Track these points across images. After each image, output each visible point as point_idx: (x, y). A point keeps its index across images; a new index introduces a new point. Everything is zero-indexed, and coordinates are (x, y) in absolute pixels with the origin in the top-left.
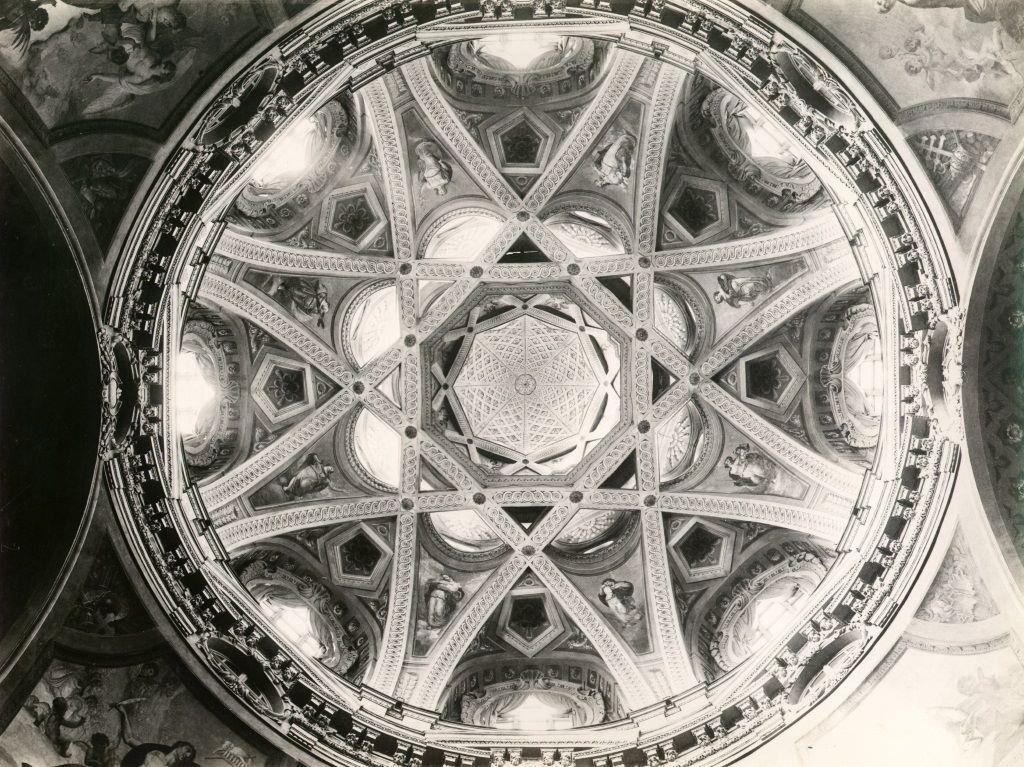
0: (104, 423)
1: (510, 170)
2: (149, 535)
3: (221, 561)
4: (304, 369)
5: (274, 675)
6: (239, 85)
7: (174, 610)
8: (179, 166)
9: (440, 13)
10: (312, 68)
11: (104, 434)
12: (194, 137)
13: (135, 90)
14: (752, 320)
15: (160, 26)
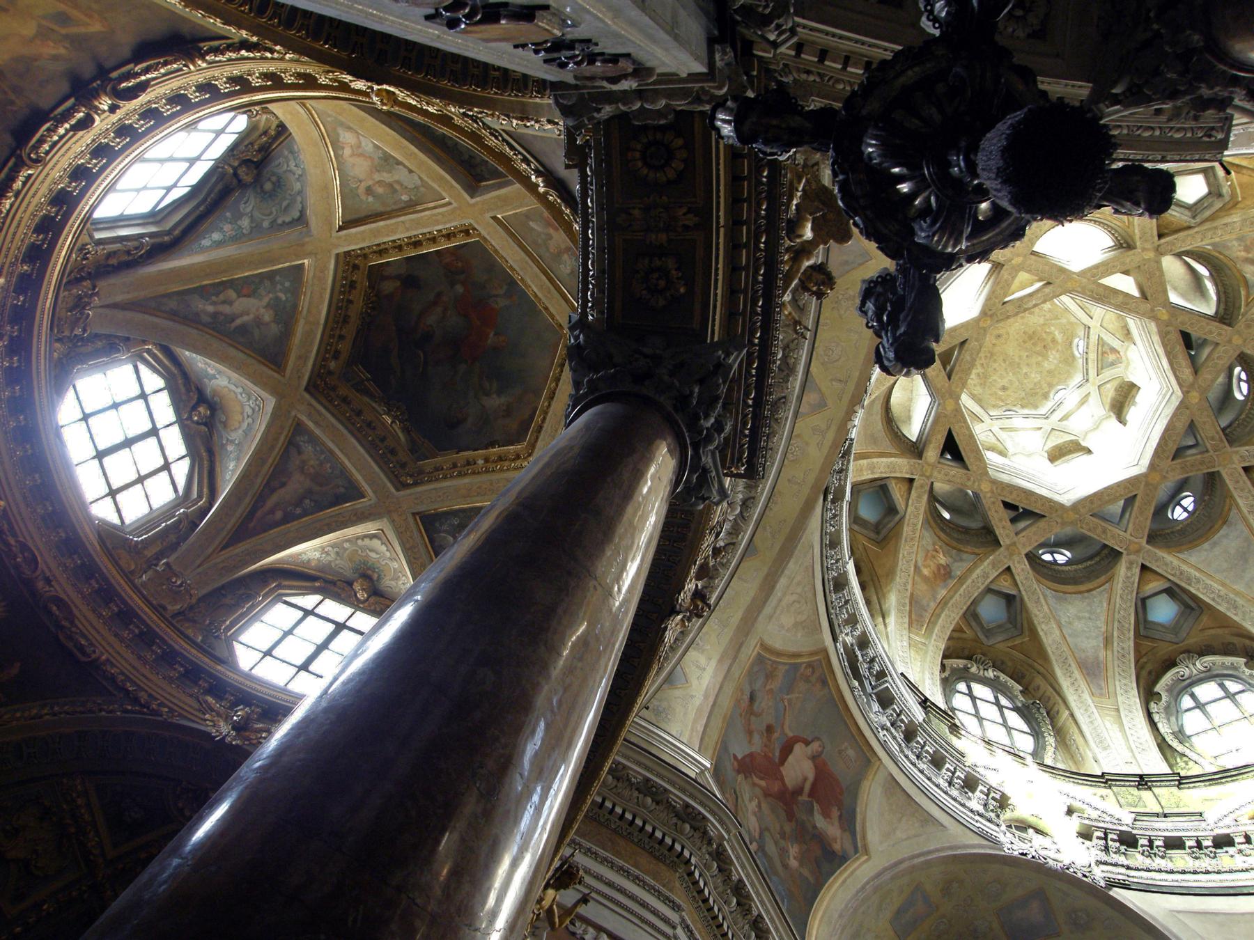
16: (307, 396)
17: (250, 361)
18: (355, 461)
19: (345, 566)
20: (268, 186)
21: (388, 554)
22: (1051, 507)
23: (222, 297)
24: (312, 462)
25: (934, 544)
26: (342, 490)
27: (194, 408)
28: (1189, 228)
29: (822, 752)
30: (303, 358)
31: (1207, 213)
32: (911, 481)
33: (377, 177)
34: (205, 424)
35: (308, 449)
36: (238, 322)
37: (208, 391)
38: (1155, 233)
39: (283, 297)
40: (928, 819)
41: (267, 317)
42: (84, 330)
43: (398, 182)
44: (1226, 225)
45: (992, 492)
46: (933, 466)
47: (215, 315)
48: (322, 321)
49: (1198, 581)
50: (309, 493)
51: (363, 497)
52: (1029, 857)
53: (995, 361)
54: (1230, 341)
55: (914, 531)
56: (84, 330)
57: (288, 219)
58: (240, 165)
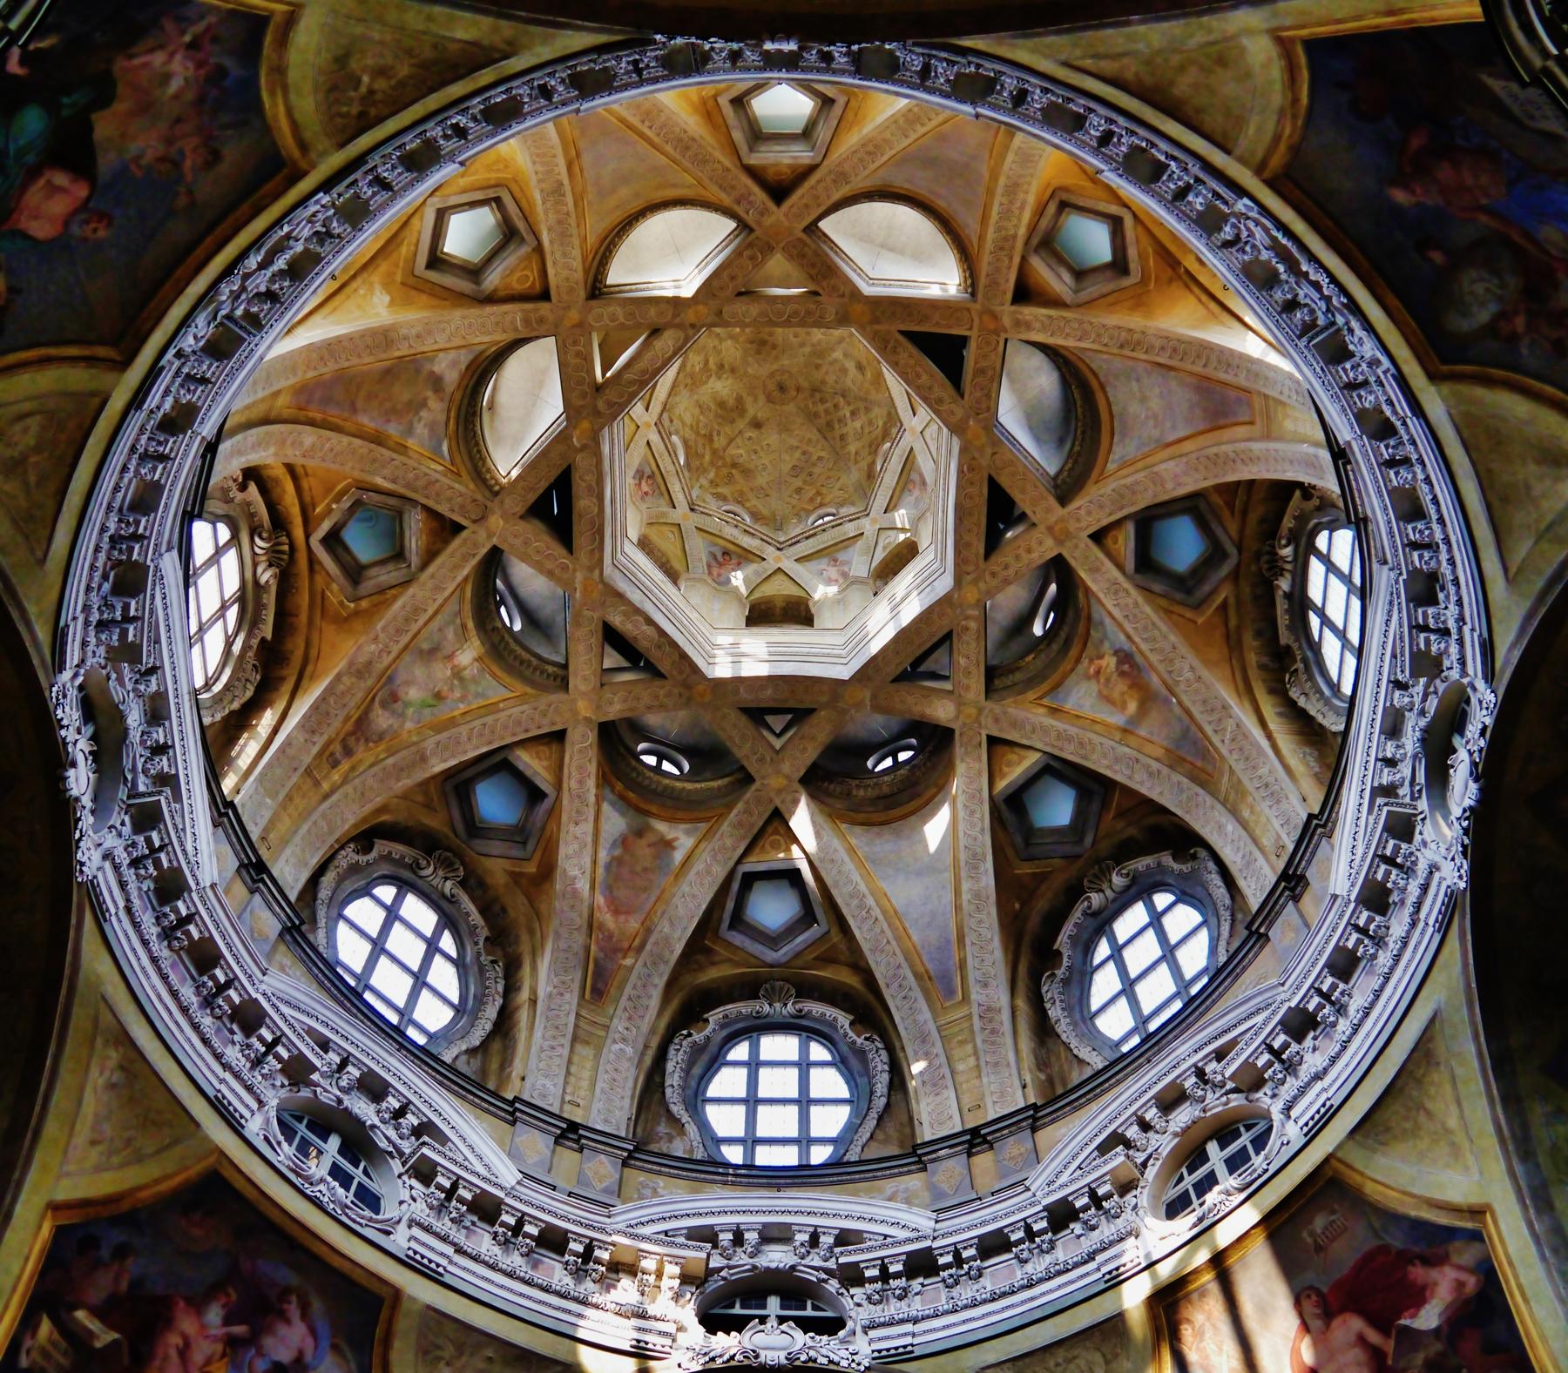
0: (815, 1361)
1: (415, 560)
2: (988, 1284)
3: (1035, 1119)
4: (745, 875)
5: (1216, 1104)
6: (307, 1179)
7: (1098, 1269)
8: (432, 1249)
9: (170, 861)
10: (270, 1047)
11: (831, 1362)
12: (388, 1233)
13: (325, 1344)
14: (669, 148)
15: (227, 1321)
22: (971, 469)
25: (1088, 677)
28: (426, 508)
29: (1319, 1293)
31: (391, 501)
32: (993, 741)
38: (457, 542)
40: (1423, 1051)
44: (394, 482)
45: (975, 582)
46: (960, 704)
49: (999, 229)
52: (1466, 841)
53: (823, 382)
54: (580, 325)
55: (1070, 739)
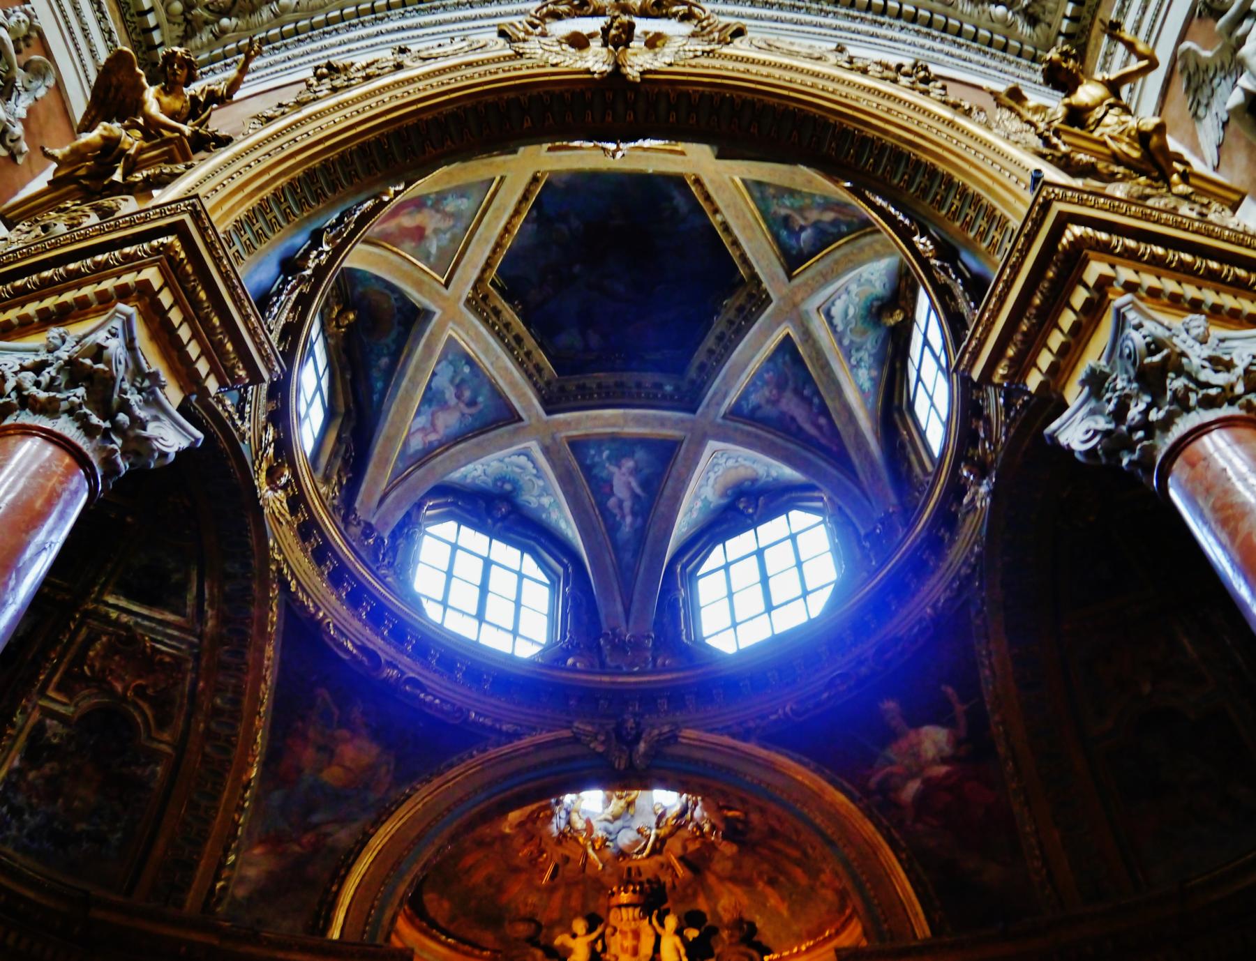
16: (700, 410)
17: (674, 472)
18: (753, 353)
19: (870, 342)
20: (508, 487)
21: (844, 297)
23: (616, 511)
24: (767, 393)
26: (787, 357)
27: (742, 513)
30: (663, 423)
33: (453, 401)
34: (757, 500)
35: (754, 399)
36: (638, 491)
37: (724, 501)
39: (606, 454)
41: (629, 464)
42: (649, 637)
43: (452, 381)
47: (634, 514)
48: (620, 411)
50: (798, 392)
51: (788, 335)
56: (649, 637)
57: (530, 465)
58: (492, 517)
